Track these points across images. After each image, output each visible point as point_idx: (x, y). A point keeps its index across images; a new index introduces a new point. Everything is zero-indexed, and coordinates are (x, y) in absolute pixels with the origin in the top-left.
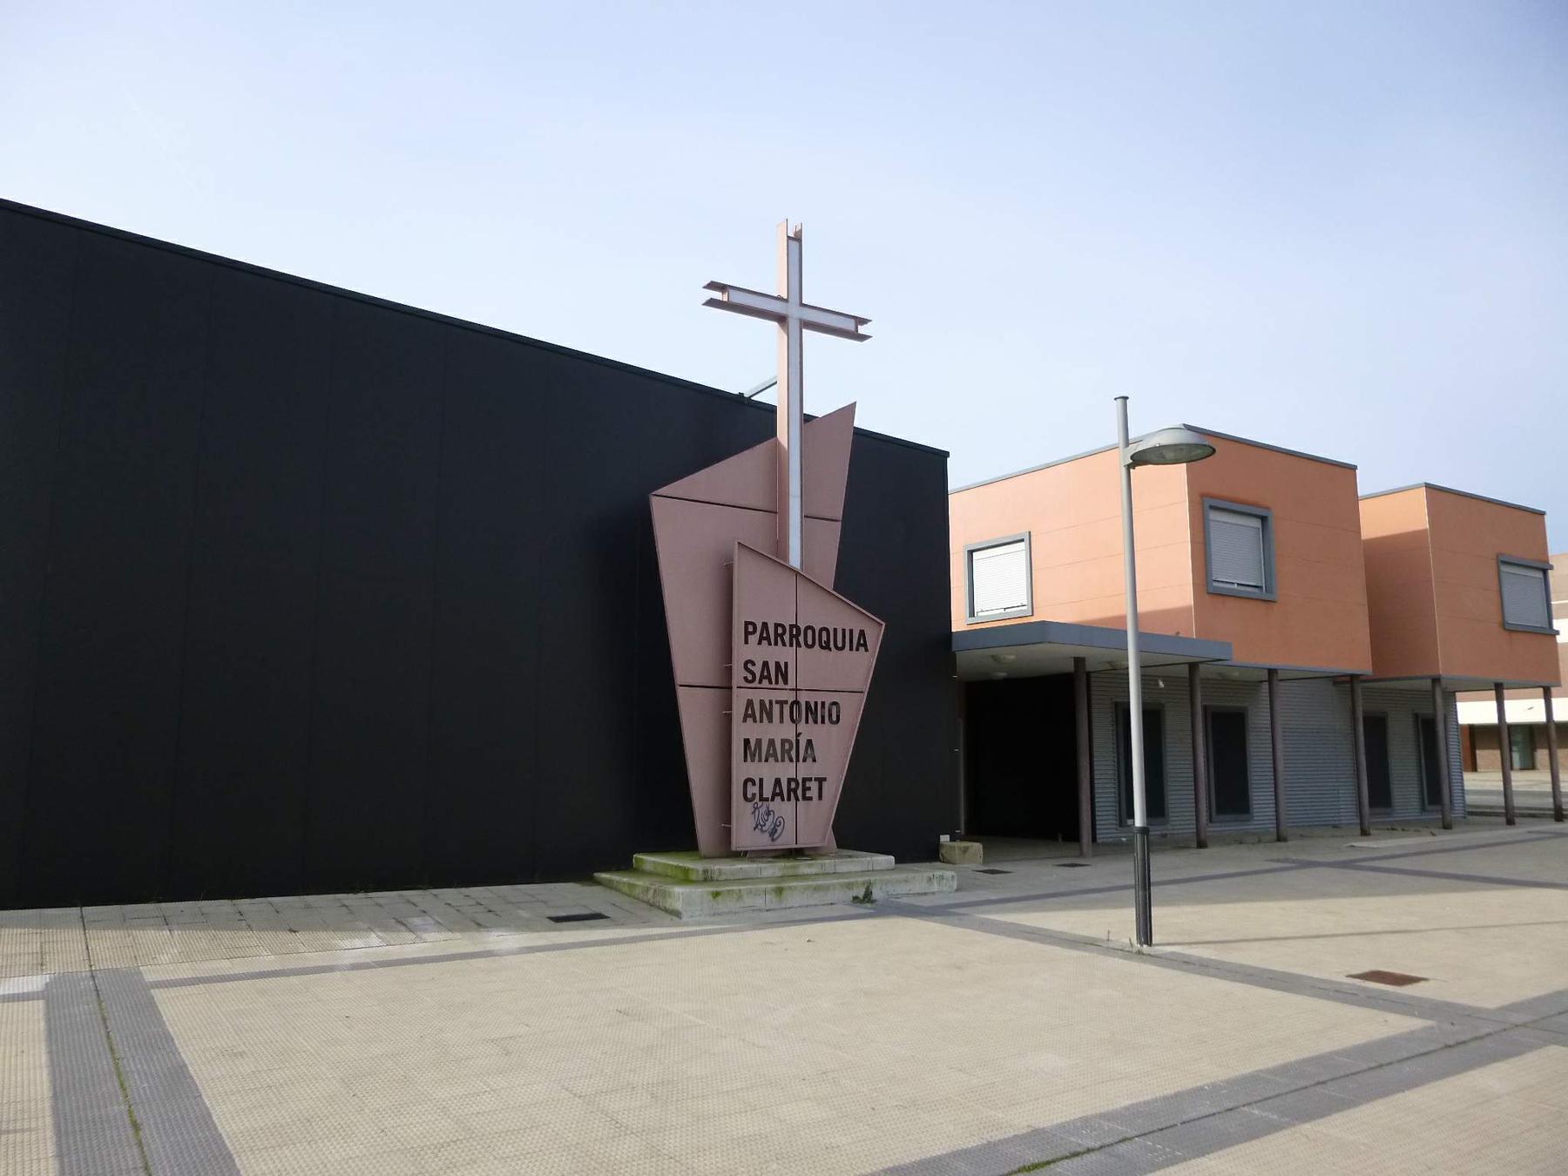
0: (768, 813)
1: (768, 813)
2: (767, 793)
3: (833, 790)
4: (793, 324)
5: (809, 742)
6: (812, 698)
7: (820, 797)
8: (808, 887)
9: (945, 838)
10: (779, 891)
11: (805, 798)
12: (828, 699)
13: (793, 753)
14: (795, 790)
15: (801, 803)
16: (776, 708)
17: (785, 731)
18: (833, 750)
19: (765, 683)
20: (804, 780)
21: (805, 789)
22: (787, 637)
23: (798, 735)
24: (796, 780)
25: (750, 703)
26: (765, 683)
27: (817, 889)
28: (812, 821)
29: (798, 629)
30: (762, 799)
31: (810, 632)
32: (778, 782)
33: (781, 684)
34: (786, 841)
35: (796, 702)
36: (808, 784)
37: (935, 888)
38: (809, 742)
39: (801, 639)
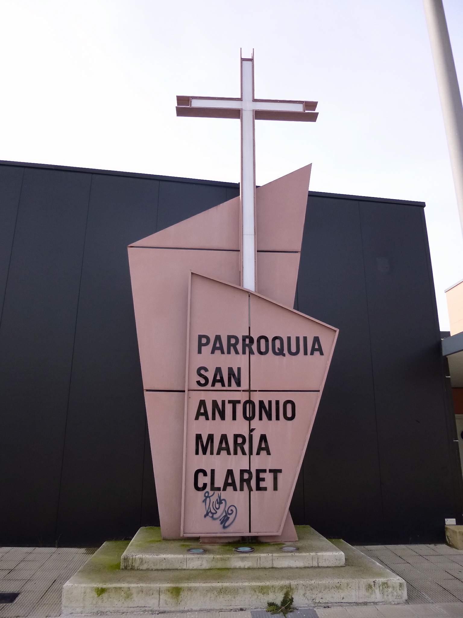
0: (220, 501)
1: (220, 501)
2: (219, 482)
3: (289, 481)
4: (248, 115)
5: (263, 438)
6: (266, 398)
7: (275, 488)
8: (212, 589)
9: (450, 522)
10: (176, 592)
11: (259, 488)
12: (283, 398)
13: (246, 447)
14: (251, 480)
15: (255, 493)
16: (229, 408)
17: (241, 427)
18: (289, 445)
19: (218, 386)
20: (258, 471)
21: (259, 480)
22: (240, 347)
23: (251, 430)
24: (249, 472)
25: (202, 403)
26: (218, 386)
27: (222, 591)
28: (271, 510)
29: (251, 340)
30: (213, 488)
31: (263, 341)
32: (230, 473)
33: (234, 386)
34: (239, 528)
35: (250, 402)
36: (262, 475)
37: (377, 596)
38: (263, 438)
39: (254, 347)
